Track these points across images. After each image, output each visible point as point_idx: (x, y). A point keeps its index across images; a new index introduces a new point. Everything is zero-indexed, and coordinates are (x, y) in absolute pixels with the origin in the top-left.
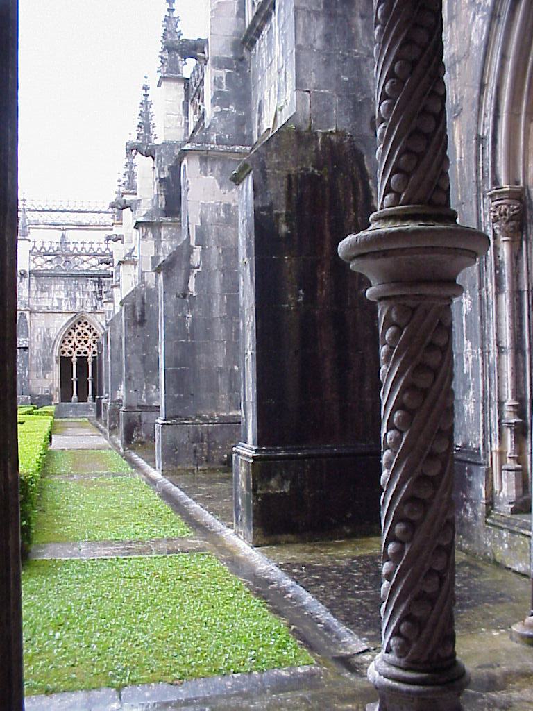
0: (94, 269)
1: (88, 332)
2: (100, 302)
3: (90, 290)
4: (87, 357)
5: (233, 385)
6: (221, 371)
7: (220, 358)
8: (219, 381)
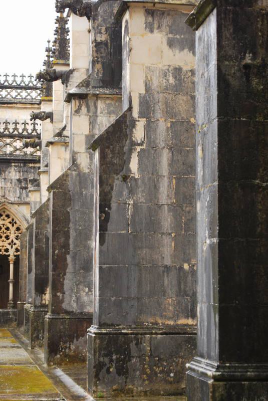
0: (18, 152)
1: (10, 226)
2: (24, 191)
3: (13, 178)
4: (9, 255)
5: (182, 287)
6: (167, 269)
7: (167, 251)
8: (166, 282)
